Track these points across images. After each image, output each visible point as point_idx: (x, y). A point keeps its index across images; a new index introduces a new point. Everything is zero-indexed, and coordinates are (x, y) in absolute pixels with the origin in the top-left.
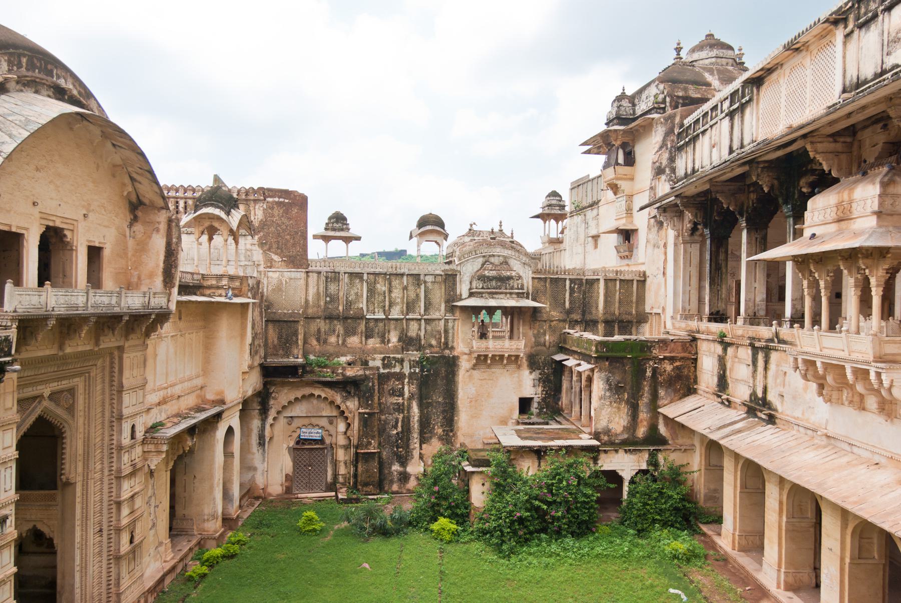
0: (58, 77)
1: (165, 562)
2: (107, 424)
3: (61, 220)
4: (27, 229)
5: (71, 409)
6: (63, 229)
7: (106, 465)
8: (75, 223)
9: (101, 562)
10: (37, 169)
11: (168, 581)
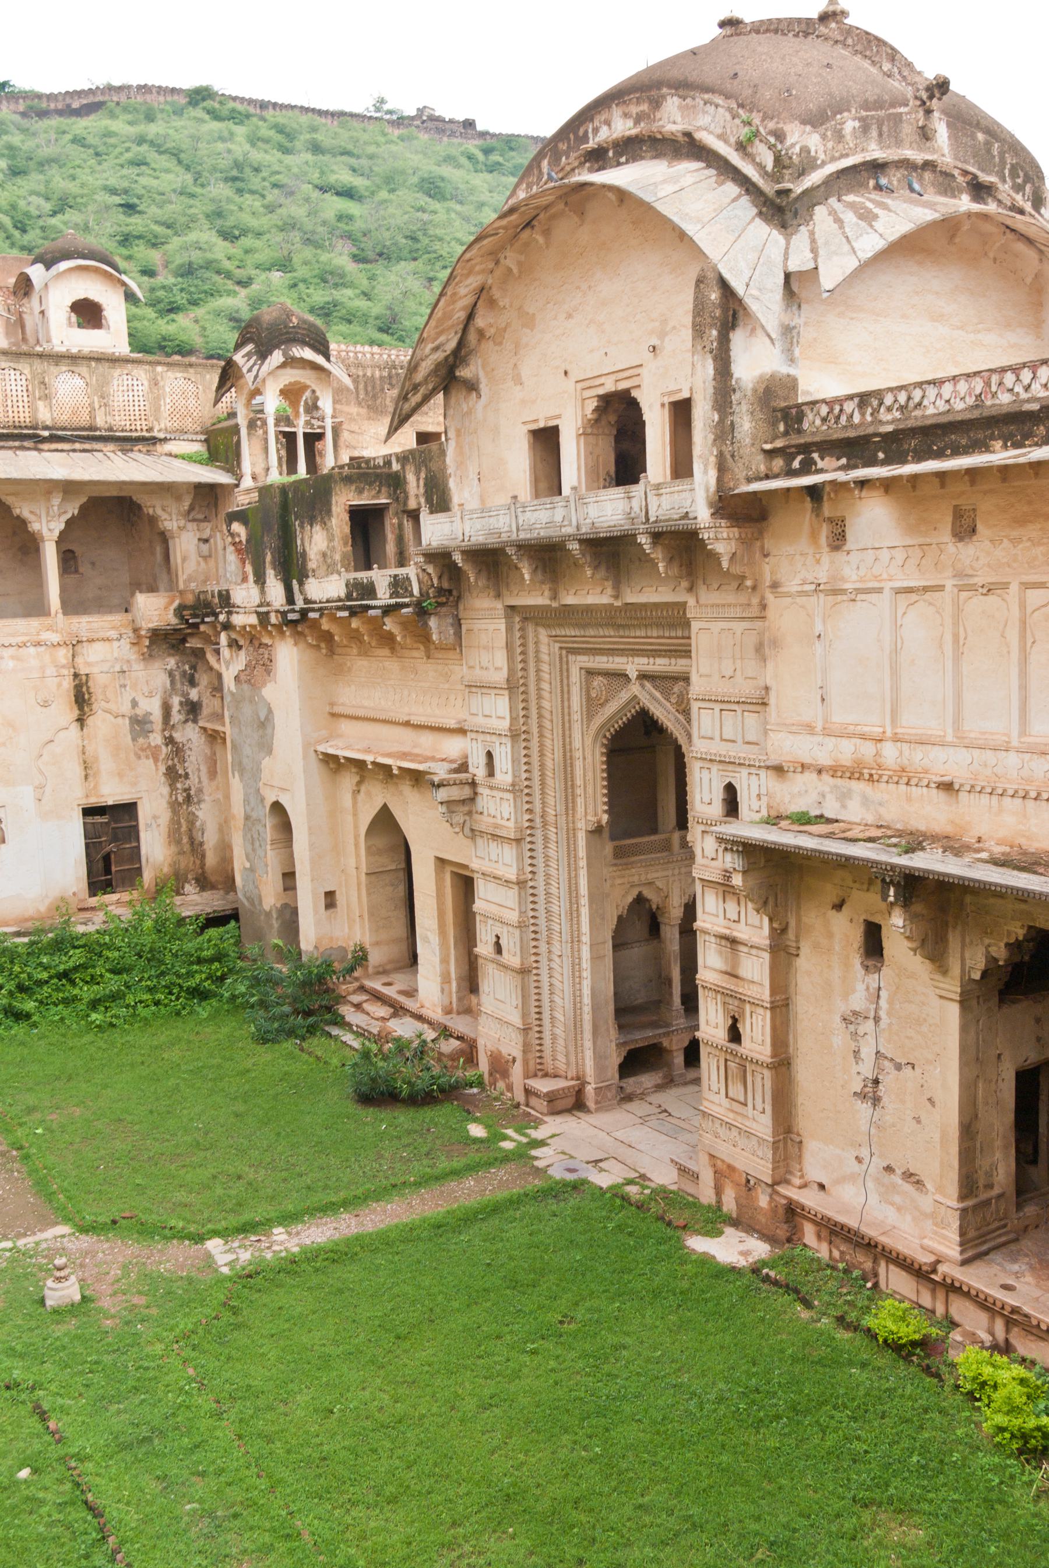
0: (596, 130)
3: (614, 377)
4: (559, 417)
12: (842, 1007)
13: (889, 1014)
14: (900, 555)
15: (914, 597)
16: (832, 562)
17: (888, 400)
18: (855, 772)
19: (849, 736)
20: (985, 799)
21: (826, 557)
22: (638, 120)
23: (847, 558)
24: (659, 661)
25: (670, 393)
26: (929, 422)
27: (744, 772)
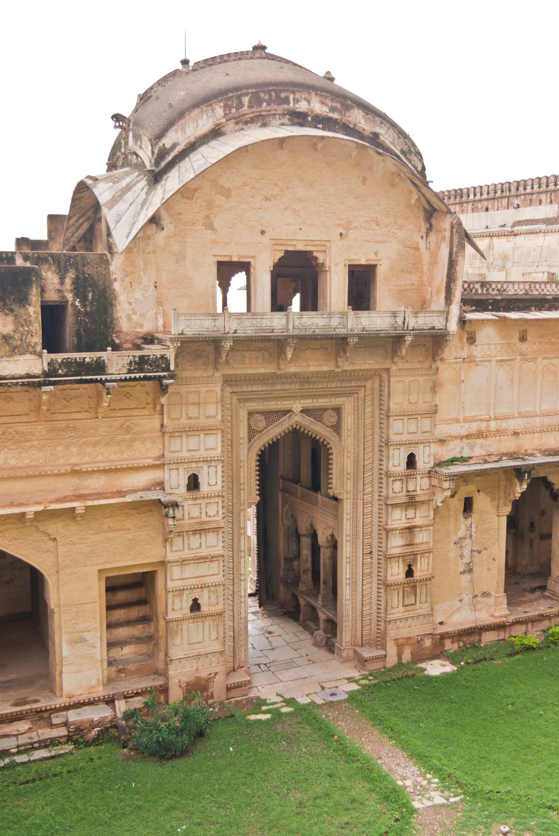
0: (296, 101)
1: (493, 616)
2: (377, 448)
4: (253, 257)
5: (337, 428)
6: (311, 252)
7: (376, 488)
8: (326, 243)
9: (371, 583)
10: (267, 199)
11: (489, 637)
12: (454, 538)
13: (476, 533)
14: (499, 347)
15: (503, 363)
16: (469, 349)
17: (494, 286)
18: (480, 435)
19: (475, 421)
20: (528, 436)
21: (466, 347)
22: (332, 109)
23: (475, 348)
24: (320, 400)
25: (350, 260)
26: (509, 297)
27: (421, 446)
